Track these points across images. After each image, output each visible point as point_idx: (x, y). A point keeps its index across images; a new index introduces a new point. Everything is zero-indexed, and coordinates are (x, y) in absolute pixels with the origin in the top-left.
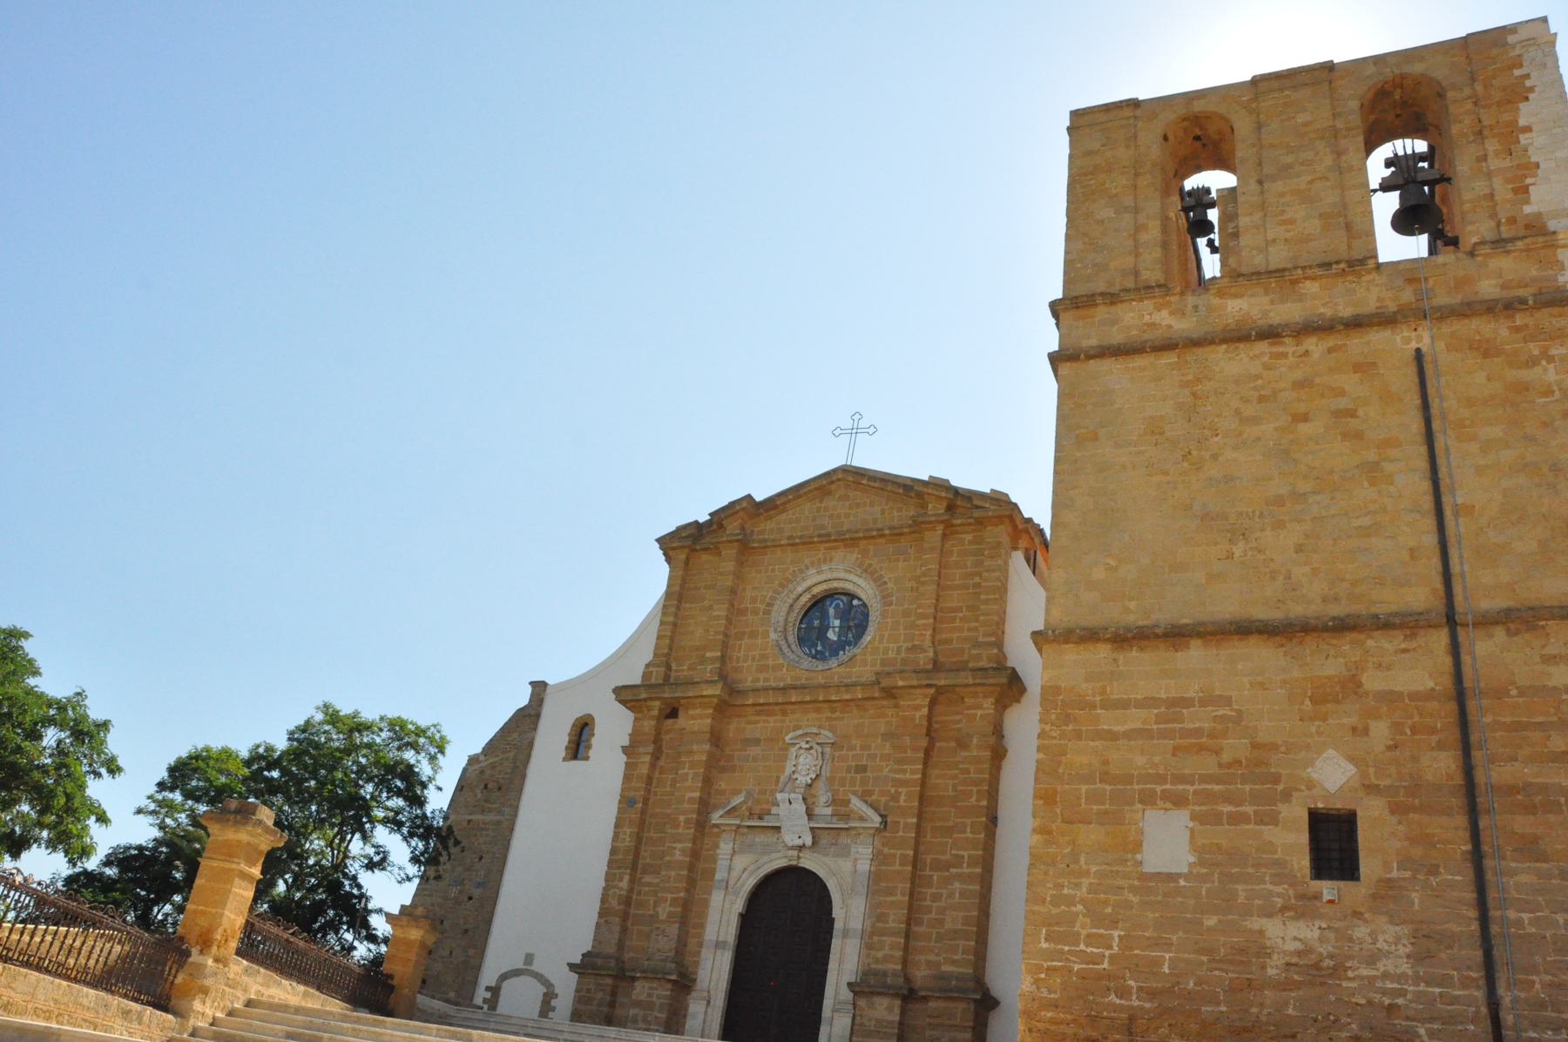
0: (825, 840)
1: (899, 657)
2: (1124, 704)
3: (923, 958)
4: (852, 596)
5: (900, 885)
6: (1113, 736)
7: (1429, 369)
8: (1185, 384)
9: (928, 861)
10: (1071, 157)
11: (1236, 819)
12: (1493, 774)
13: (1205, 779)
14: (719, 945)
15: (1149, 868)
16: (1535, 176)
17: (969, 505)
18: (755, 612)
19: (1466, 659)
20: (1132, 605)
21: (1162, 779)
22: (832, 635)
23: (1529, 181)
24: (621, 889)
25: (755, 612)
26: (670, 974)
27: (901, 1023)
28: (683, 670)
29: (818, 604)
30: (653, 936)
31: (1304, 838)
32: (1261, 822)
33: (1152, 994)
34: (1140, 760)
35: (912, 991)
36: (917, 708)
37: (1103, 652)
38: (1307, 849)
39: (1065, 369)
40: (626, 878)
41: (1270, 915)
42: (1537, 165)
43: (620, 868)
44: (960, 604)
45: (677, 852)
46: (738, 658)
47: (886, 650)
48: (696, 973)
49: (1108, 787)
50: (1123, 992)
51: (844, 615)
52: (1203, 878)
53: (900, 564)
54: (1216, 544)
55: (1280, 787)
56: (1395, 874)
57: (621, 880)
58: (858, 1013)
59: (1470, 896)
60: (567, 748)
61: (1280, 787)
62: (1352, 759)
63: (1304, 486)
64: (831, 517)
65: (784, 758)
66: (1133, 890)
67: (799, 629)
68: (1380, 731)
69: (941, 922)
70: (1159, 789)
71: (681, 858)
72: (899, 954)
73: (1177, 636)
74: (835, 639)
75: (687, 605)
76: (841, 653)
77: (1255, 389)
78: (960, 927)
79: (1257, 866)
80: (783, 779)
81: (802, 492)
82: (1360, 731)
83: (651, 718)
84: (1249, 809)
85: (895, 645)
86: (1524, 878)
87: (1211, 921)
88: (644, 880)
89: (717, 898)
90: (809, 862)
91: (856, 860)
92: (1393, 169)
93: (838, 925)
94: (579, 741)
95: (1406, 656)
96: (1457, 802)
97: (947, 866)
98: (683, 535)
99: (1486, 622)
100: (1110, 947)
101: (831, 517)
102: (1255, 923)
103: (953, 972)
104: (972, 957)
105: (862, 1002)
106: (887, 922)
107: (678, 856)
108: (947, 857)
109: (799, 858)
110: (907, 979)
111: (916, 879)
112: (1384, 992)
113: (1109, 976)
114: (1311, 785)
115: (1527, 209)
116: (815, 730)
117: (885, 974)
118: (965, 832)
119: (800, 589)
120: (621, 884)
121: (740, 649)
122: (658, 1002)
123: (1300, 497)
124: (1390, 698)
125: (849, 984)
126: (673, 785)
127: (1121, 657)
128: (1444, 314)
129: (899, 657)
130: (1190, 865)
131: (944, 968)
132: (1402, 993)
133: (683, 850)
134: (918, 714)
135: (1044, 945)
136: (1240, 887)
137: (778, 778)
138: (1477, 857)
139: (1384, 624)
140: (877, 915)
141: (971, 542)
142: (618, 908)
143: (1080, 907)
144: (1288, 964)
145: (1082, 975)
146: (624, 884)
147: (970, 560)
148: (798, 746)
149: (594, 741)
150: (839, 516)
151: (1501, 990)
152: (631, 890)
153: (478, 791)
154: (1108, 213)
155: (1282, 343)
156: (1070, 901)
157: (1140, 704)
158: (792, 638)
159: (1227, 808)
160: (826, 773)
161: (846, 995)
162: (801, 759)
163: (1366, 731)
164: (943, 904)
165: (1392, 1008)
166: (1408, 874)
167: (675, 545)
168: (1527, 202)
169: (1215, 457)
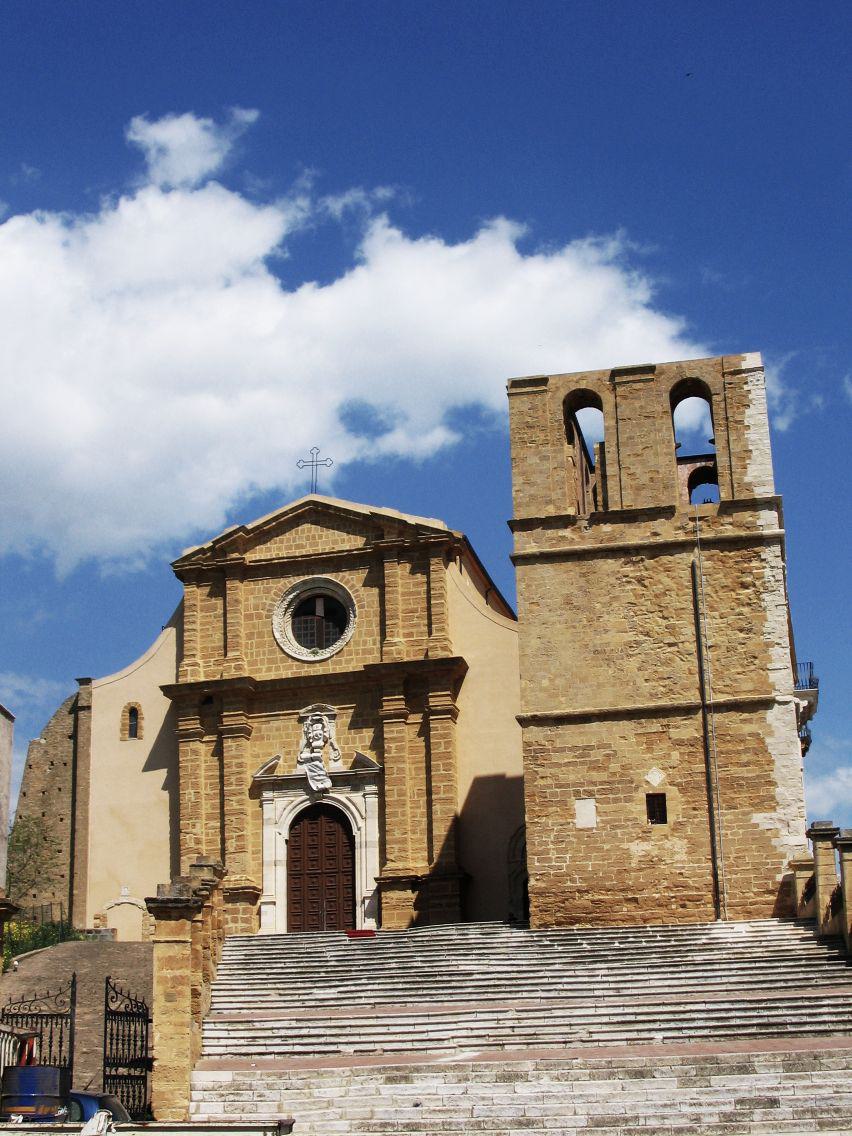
2: (562, 750)
6: (558, 765)
7: (698, 572)
8: (583, 575)
11: (616, 800)
12: (717, 774)
13: (601, 783)
15: (578, 826)
16: (750, 458)
18: (259, 617)
23: (748, 462)
25: (259, 617)
31: (644, 807)
42: (751, 451)
43: (191, 818)
46: (252, 653)
47: (365, 643)
50: (573, 881)
55: (633, 785)
61: (633, 785)
66: (573, 836)
68: (675, 755)
70: (581, 789)
71: (238, 807)
85: (371, 639)
86: (729, 817)
87: (606, 847)
89: (269, 831)
101: (308, 538)
102: (625, 846)
104: (453, 851)
112: (676, 868)
115: (747, 479)
120: (194, 831)
124: (680, 743)
128: (706, 544)
132: (683, 868)
136: (618, 831)
138: (711, 810)
143: (551, 846)
145: (556, 875)
151: (719, 863)
153: (46, 767)
154: (534, 460)
156: (546, 843)
157: (570, 749)
159: (611, 796)
165: (681, 874)
168: (745, 474)
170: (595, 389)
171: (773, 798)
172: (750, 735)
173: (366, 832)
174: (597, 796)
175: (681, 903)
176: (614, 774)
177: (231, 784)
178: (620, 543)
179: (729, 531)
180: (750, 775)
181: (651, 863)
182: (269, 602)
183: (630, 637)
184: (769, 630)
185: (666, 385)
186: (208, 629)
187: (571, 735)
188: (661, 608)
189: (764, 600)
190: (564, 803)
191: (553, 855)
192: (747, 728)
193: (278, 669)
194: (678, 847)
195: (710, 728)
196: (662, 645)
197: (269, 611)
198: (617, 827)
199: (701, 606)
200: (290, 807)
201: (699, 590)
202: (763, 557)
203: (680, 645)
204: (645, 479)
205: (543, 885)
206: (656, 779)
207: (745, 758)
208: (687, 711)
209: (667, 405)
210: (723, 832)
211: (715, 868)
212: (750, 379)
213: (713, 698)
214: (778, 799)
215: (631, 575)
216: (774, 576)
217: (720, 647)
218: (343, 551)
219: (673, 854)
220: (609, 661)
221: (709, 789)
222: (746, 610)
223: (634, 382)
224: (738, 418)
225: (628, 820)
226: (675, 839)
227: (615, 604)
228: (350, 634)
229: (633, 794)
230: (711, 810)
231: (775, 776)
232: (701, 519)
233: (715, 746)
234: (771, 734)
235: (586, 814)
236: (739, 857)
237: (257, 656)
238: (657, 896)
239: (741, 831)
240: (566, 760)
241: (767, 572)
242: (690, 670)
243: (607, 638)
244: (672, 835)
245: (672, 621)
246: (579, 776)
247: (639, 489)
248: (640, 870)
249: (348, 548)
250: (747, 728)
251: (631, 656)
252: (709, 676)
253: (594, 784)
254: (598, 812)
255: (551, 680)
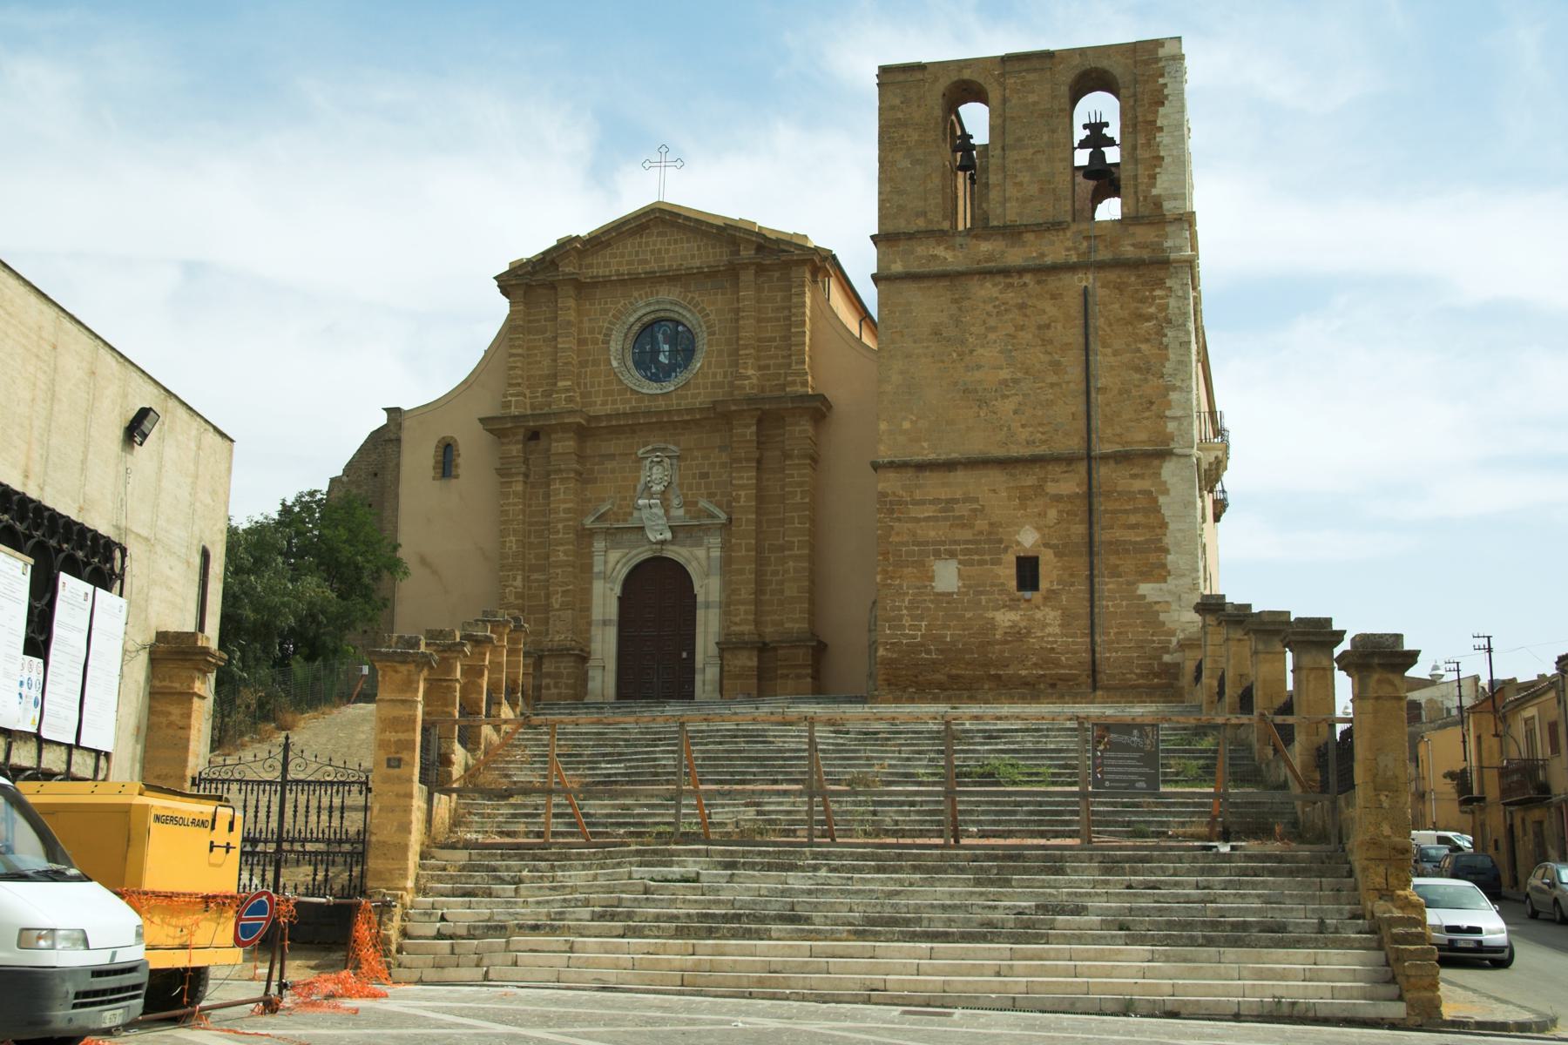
0: (681, 535)
1: (726, 380)
3: (769, 618)
4: (678, 323)
5: (748, 567)
6: (917, 520)
7: (1090, 299)
8: (955, 301)
9: (766, 546)
10: (880, 109)
11: (982, 563)
12: (1102, 536)
13: (967, 542)
14: (605, 623)
15: (935, 590)
16: (1161, 166)
17: (776, 247)
18: (595, 342)
19: (1095, 475)
20: (925, 445)
21: (943, 543)
22: (663, 358)
24: (516, 588)
25: (595, 342)
26: (573, 649)
27: (758, 668)
28: (537, 397)
29: (648, 329)
30: (551, 622)
31: (1014, 571)
32: (992, 564)
33: (941, 651)
34: (932, 534)
35: (765, 644)
36: (747, 426)
37: (910, 473)
38: (1015, 577)
39: (883, 285)
40: (519, 578)
41: (998, 610)
42: (1163, 158)
43: (511, 570)
44: (774, 335)
45: (561, 554)
46: (585, 384)
47: (714, 375)
48: (588, 646)
49: (916, 548)
50: (928, 652)
51: (673, 340)
52: (966, 594)
53: (719, 297)
54: (971, 408)
55: (1002, 546)
56: (1055, 587)
57: (515, 579)
58: (725, 663)
59: (1087, 596)
60: (434, 468)
61: (1002, 546)
62: (1038, 529)
63: (1019, 375)
64: (652, 252)
65: (638, 470)
66: (931, 601)
67: (634, 353)
68: (1052, 514)
69: (782, 591)
70: (942, 548)
71: (565, 558)
72: (751, 617)
73: (950, 466)
74: (667, 362)
75: (532, 337)
76: (673, 374)
77: (994, 307)
78: (796, 594)
79: (992, 586)
80: (639, 487)
81: (624, 229)
82: (1043, 515)
83: (517, 442)
84: (987, 557)
86: (1111, 586)
87: (968, 615)
88: (532, 578)
89: (598, 587)
90: (672, 552)
91: (709, 548)
92: (1087, 132)
93: (700, 599)
94: (446, 460)
95: (1066, 475)
96: (1084, 550)
97: (782, 548)
98: (520, 273)
99: (1105, 458)
100: (920, 630)
101: (652, 252)
102: (990, 615)
103: (793, 628)
104: (806, 616)
105: (727, 655)
106: (740, 595)
107: (562, 557)
108: (781, 542)
109: (662, 549)
110: (760, 635)
111: (761, 561)
112: (1048, 642)
113: (922, 645)
114: (1018, 543)
115: (1155, 192)
116: (663, 445)
117: (743, 634)
118: (794, 523)
119: (632, 320)
120: (515, 584)
121: (586, 375)
122: (565, 672)
123: (1016, 381)
124: (1058, 498)
125: (717, 643)
126: (547, 496)
127: (921, 475)
128: (1101, 266)
129: (726, 380)
130: (959, 587)
131: (786, 626)
132: (1056, 642)
133: (565, 553)
134: (749, 431)
135: (888, 632)
137: (635, 487)
138: (1091, 577)
139: (1056, 459)
140: (728, 587)
141: (778, 279)
142: (516, 602)
143: (905, 612)
144: (1006, 633)
145: (908, 645)
146: (519, 582)
147: (779, 295)
148: (650, 460)
149: (460, 461)
150: (659, 251)
151: (1098, 639)
152: (524, 586)
154: (906, 163)
155: (1012, 277)
156: (900, 609)
157: (933, 502)
158: (630, 364)
159: (976, 557)
160: (676, 480)
161: (713, 650)
162: (654, 470)
163: (1045, 514)
164: (780, 577)
165: (1053, 649)
166: (1060, 587)
167: (513, 282)
168: (1154, 185)
169: (971, 352)
170: (981, 81)
171: (1164, 566)
172: (1140, 492)
173: (708, 588)
174: (960, 557)
175: (1052, 682)
176: (981, 533)
177: (558, 532)
178: (1001, 264)
179: (1128, 250)
180: (1138, 539)
181: (1018, 635)
182: (606, 325)
183: (1004, 374)
184: (1171, 371)
185: (1066, 77)
186: (536, 355)
187: (935, 486)
188: (1046, 342)
189: (1166, 335)
190: (921, 564)
191: (907, 622)
192: (1138, 485)
193: (614, 402)
194: (1050, 616)
195: (1095, 483)
196: (1043, 385)
197: (606, 335)
198: (981, 593)
199: (1091, 339)
200: (624, 560)
201: (1091, 322)
202: (1167, 285)
203: (1064, 386)
204: (1033, 189)
205: (895, 656)
206: (1028, 539)
207: (1133, 519)
208: (1068, 460)
209: (1066, 101)
210: (1104, 603)
211: (1093, 642)
212: (1167, 70)
213: (1101, 448)
214: (1169, 567)
215: (1011, 302)
216: (1179, 308)
217: (1111, 389)
218: (692, 268)
219: (1044, 626)
220: (982, 402)
221: (1091, 553)
222: (1143, 347)
223: (1027, 71)
224: (1150, 118)
225: (995, 586)
226: (1047, 609)
227: (992, 336)
228: (699, 365)
229: (1002, 556)
230: (1091, 577)
231: (1168, 540)
232: (1095, 237)
233: (1101, 505)
234: (1166, 492)
235: (947, 577)
236: (1121, 633)
237: (592, 386)
238: (1023, 673)
239: (1124, 603)
240: (926, 515)
241: (1172, 302)
242: (1073, 414)
243: (978, 375)
244: (1044, 605)
245: (1057, 357)
246: (941, 533)
247: (1025, 201)
248: (1006, 642)
249: (698, 265)
250: (1138, 485)
251: (1008, 397)
252: (1097, 422)
253: (956, 542)
254: (960, 576)
255: (912, 422)
